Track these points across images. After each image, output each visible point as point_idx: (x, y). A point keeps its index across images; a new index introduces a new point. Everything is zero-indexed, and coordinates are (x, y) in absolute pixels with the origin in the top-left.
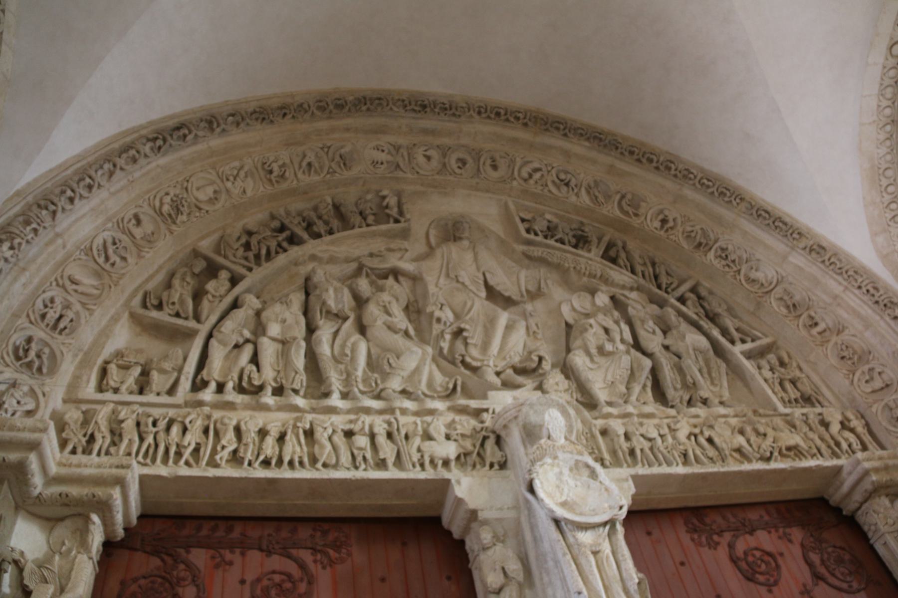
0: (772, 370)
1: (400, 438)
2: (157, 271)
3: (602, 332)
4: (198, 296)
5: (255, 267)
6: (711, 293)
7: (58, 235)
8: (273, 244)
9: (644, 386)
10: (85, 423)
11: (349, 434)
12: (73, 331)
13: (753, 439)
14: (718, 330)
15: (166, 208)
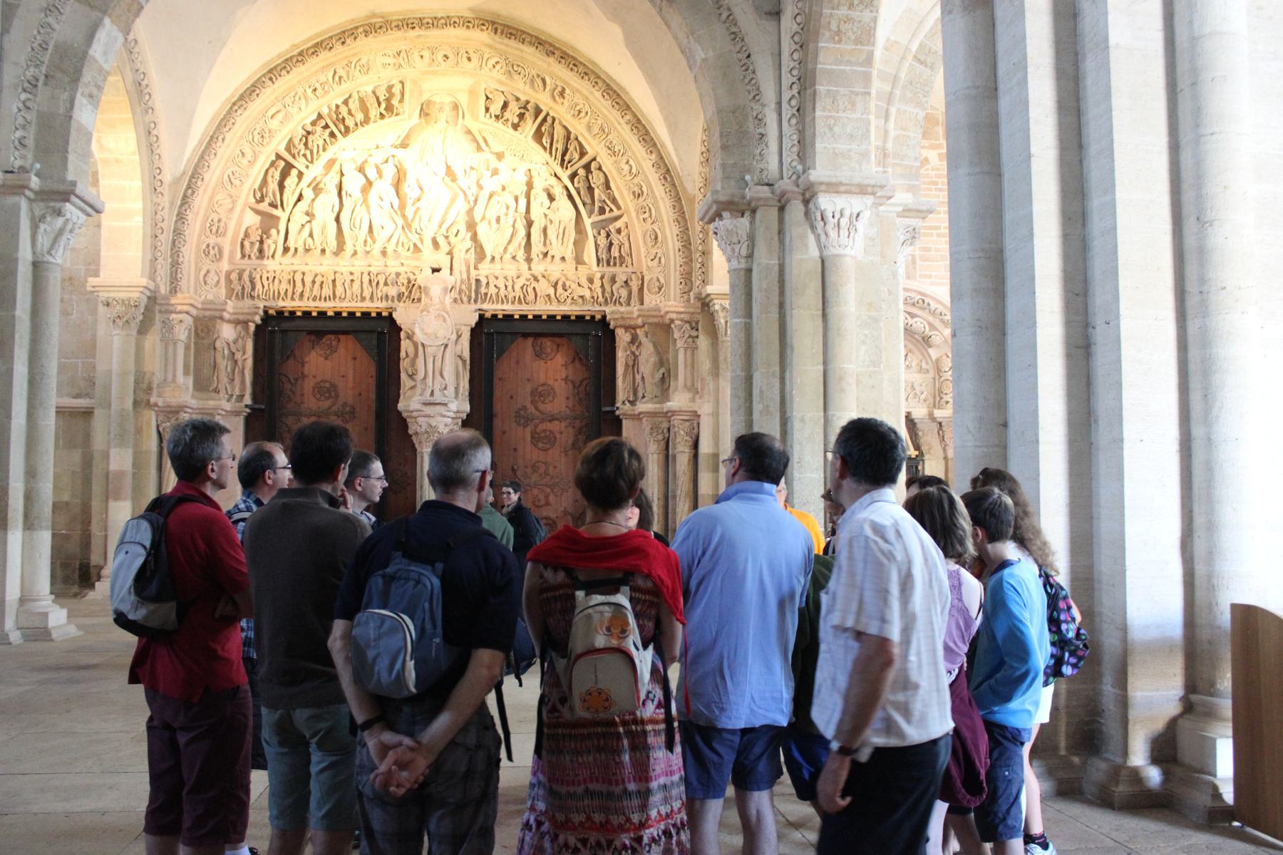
0: (608, 236)
1: (374, 284)
2: (259, 174)
3: (505, 207)
4: (281, 186)
5: (310, 165)
6: (600, 169)
7: (207, 185)
8: (321, 143)
9: (520, 245)
10: (240, 279)
11: (352, 281)
12: (226, 231)
13: (560, 289)
14: (588, 201)
15: (257, 137)
